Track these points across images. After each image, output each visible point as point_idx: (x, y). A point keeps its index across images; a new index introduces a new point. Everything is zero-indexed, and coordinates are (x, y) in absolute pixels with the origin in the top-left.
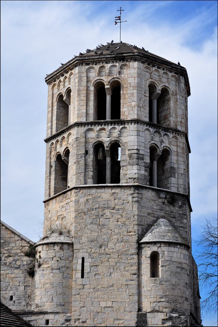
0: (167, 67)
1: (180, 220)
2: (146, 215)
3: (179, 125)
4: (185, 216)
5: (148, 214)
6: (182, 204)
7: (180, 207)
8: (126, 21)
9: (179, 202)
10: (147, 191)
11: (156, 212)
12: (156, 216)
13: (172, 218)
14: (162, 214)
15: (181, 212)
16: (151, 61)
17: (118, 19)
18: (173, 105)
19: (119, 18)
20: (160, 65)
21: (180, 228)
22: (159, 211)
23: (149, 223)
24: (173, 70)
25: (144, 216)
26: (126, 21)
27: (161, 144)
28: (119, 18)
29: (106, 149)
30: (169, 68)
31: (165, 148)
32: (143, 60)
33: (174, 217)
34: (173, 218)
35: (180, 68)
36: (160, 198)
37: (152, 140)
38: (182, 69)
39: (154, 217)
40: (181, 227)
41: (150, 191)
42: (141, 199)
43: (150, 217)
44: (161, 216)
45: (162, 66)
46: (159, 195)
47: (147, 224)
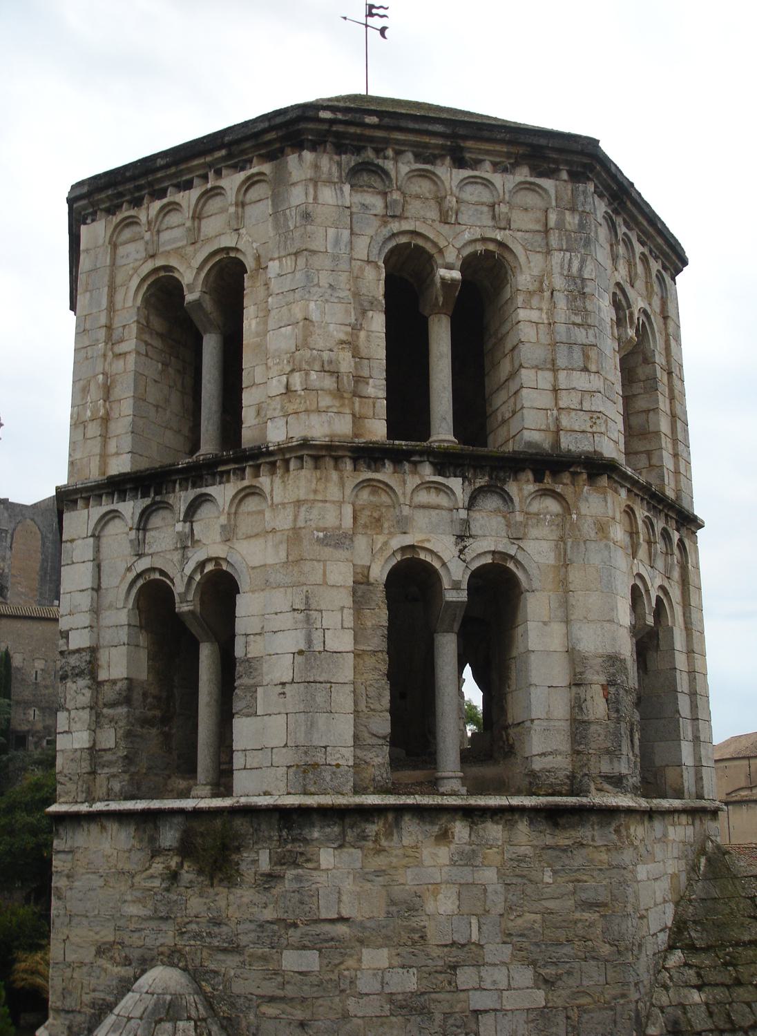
0: (209, 159)
1: (264, 958)
2: (88, 955)
3: (277, 413)
4: (291, 931)
5: (100, 952)
6: (280, 861)
7: (271, 878)
8: (345, 18)
9: (257, 853)
10: (94, 828)
11: (136, 935)
12: (135, 954)
13: (221, 956)
14: (168, 937)
15: (269, 914)
16: (130, 186)
17: (378, 8)
18: (257, 323)
19: (374, 11)
20: (180, 173)
21: (264, 1009)
22: (153, 924)
23: (102, 995)
24: (243, 152)
25: (82, 964)
26: (345, 18)
27: (184, 559)
28: (374, 11)
29: (183, 608)
30: (224, 159)
31: (209, 567)
32: (102, 201)
33: (233, 948)
34: (225, 950)
35: (266, 124)
36: (156, 853)
37: (140, 556)
38: (278, 120)
39: (127, 962)
40: (272, 999)
41: (113, 827)
42: (68, 877)
43: (108, 966)
44: (162, 953)
45: (190, 170)
46: (152, 840)
47: (93, 1005)
